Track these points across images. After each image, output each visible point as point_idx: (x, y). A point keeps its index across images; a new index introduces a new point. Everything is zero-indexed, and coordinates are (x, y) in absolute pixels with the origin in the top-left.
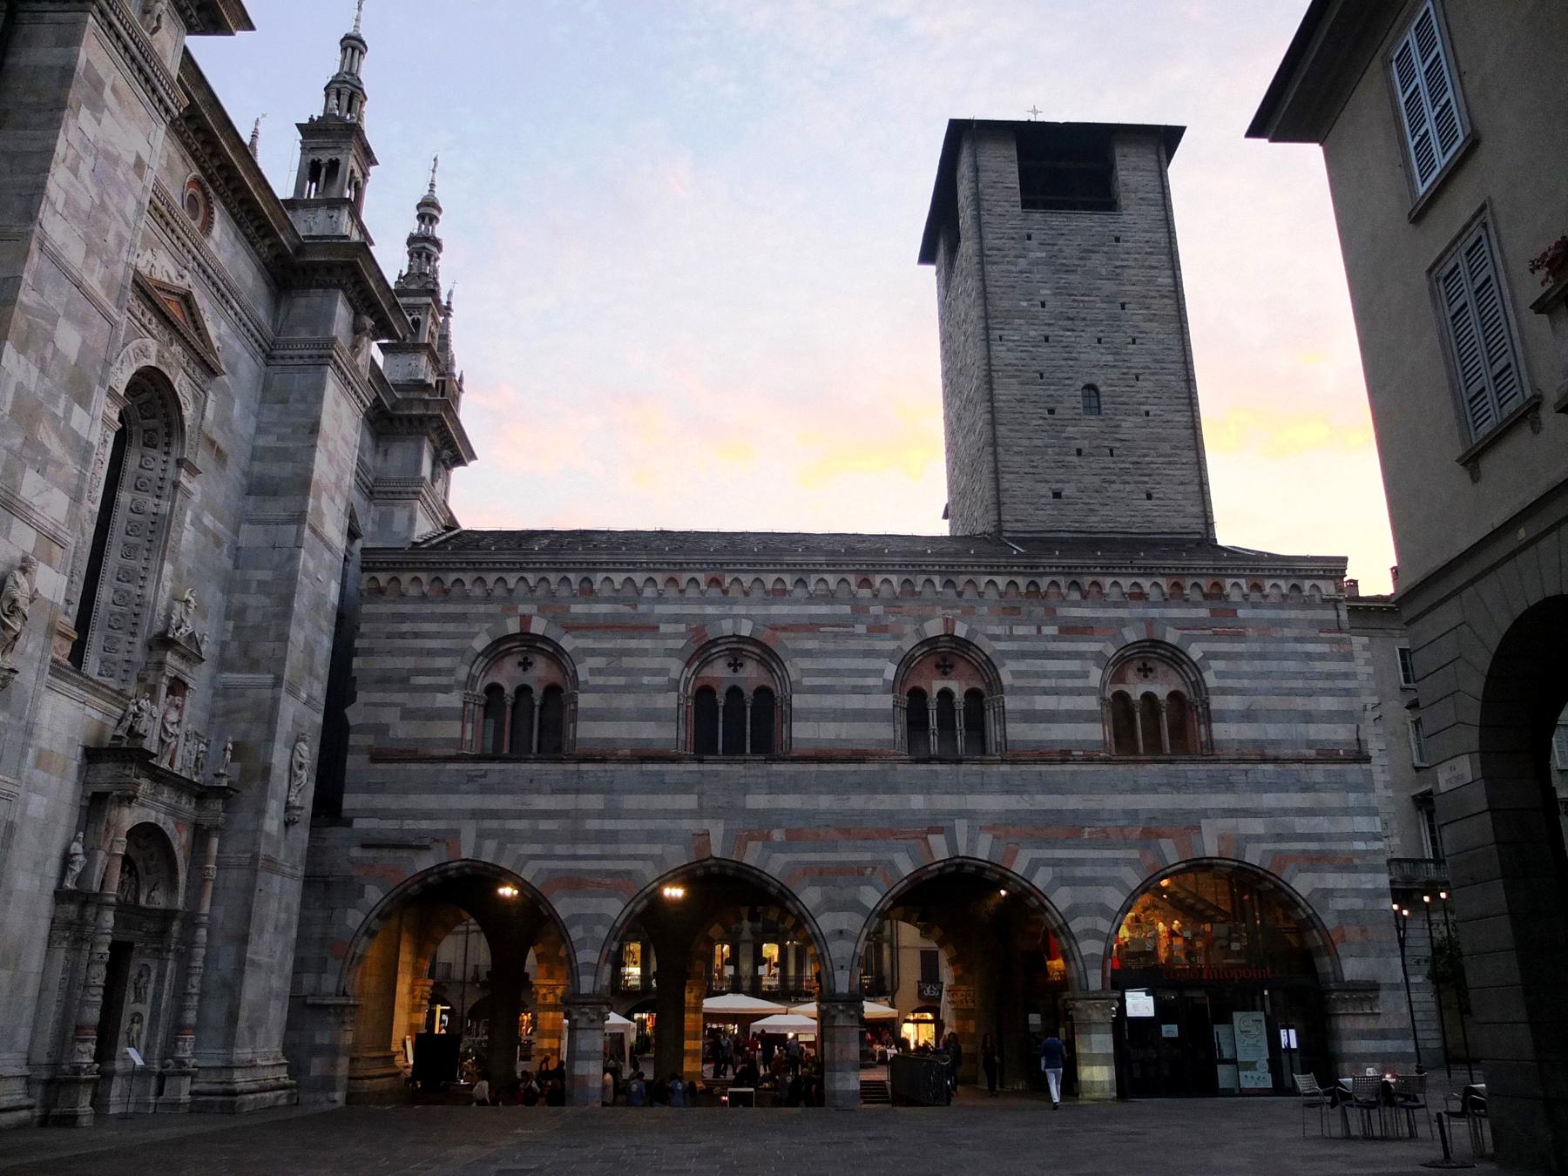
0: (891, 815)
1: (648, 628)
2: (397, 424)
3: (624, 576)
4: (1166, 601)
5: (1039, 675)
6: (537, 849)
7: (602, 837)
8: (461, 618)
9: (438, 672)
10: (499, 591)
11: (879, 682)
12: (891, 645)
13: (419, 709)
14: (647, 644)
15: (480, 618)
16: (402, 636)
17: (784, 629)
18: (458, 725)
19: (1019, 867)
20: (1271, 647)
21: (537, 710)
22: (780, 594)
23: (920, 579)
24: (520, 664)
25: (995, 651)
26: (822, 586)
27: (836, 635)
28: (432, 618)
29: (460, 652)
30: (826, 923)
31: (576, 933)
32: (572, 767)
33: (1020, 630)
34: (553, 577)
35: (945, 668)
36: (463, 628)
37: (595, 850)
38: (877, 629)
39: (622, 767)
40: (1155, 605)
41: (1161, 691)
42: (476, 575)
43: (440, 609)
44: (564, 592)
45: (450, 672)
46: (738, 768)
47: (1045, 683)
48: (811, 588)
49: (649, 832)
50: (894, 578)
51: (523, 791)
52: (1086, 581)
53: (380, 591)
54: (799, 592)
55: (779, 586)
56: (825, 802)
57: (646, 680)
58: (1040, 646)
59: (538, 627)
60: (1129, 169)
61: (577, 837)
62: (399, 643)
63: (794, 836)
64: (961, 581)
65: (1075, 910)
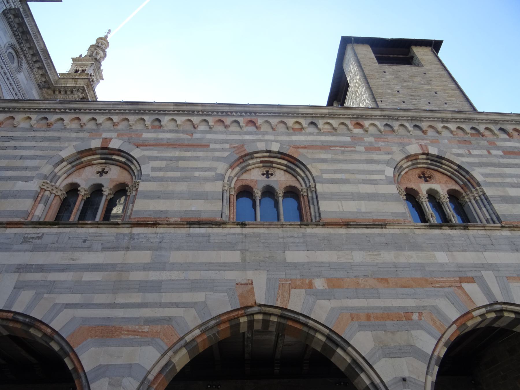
0: (421, 267)
2: (57, 93)
3: (185, 118)
7: (144, 287)
11: (384, 177)
14: (200, 154)
15: (69, 140)
17: (305, 147)
24: (98, 172)
25: (462, 162)
27: (343, 152)
28: (34, 139)
33: (475, 152)
34: (132, 118)
35: (425, 178)
36: (57, 144)
37: (137, 298)
39: (171, 230)
49: (193, 281)
51: (74, 249)
56: (358, 257)
57: (197, 174)
59: (115, 144)
60: (421, 53)
61: (119, 287)
63: (334, 284)
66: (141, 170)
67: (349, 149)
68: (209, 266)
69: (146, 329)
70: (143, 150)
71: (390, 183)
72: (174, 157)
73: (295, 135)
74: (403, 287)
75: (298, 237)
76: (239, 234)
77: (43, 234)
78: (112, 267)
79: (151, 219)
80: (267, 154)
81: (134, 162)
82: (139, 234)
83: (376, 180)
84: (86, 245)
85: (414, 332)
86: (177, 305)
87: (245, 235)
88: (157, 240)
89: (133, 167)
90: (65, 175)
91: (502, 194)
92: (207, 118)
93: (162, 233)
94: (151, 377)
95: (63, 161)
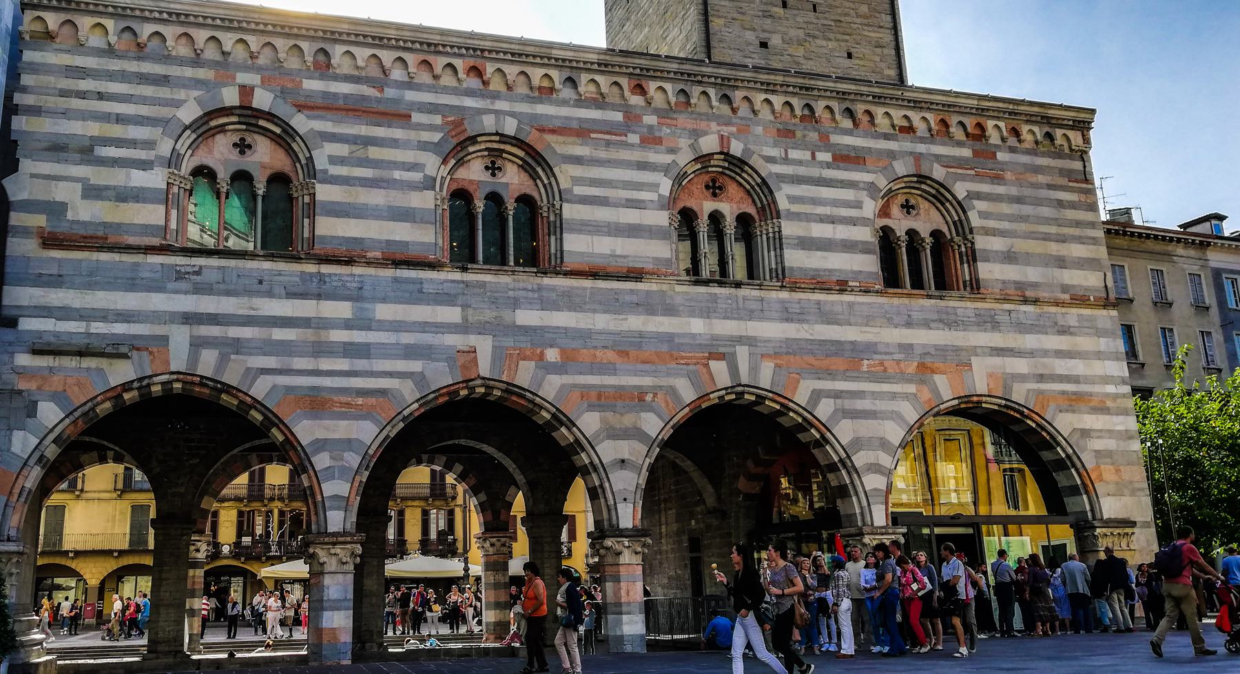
0: (669, 338)
1: (400, 116)
3: (369, 52)
4: (932, 137)
5: (815, 201)
6: (271, 362)
7: (350, 350)
8: (164, 80)
9: (132, 143)
10: (211, 53)
12: (667, 159)
13: (107, 188)
14: (398, 133)
16: (82, 95)
17: (553, 131)
18: (162, 208)
19: (801, 396)
20: (1027, 192)
21: (260, 200)
22: (547, 92)
23: (696, 91)
25: (770, 174)
26: (592, 88)
28: (123, 76)
29: (163, 123)
30: (607, 451)
31: (321, 461)
32: (311, 268)
33: (794, 154)
35: (715, 189)
36: (164, 93)
37: (342, 364)
38: (651, 140)
39: (371, 271)
40: (922, 140)
41: (924, 230)
42: (180, 30)
43: (133, 66)
44: (293, 63)
45: (149, 144)
46: (505, 279)
47: (820, 210)
48: (581, 89)
49: (407, 346)
50: (668, 86)
51: (249, 293)
52: (860, 108)
53: (49, 36)
54: (567, 93)
55: (546, 84)
56: (601, 321)
57: (397, 175)
58: (815, 172)
59: (262, 100)
61: (321, 349)
62: (76, 103)
64: (738, 95)
65: (858, 444)
66: (311, 157)
67: (618, 138)
68: (424, 327)
69: (360, 401)
70: (308, 117)
71: (662, 208)
72: (360, 136)
73: (541, 102)
74: (644, 362)
75: (533, 290)
76: (458, 282)
77: (201, 267)
78: (304, 323)
79: (342, 250)
80: (497, 138)
81: (298, 138)
82: (330, 275)
83: (643, 201)
84: (263, 288)
85: (643, 415)
86: (390, 374)
87: (467, 284)
88: (355, 285)
89: (294, 146)
90: (190, 152)
91: (801, 233)
92: (405, 55)
93: (360, 276)
94: (371, 452)
95: (186, 128)
